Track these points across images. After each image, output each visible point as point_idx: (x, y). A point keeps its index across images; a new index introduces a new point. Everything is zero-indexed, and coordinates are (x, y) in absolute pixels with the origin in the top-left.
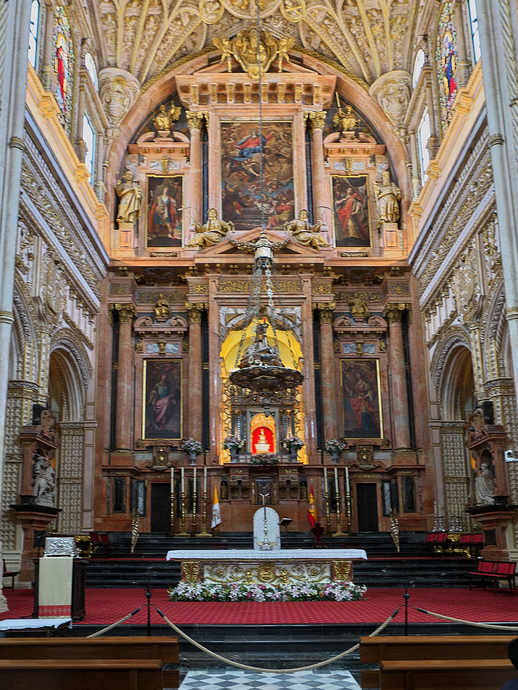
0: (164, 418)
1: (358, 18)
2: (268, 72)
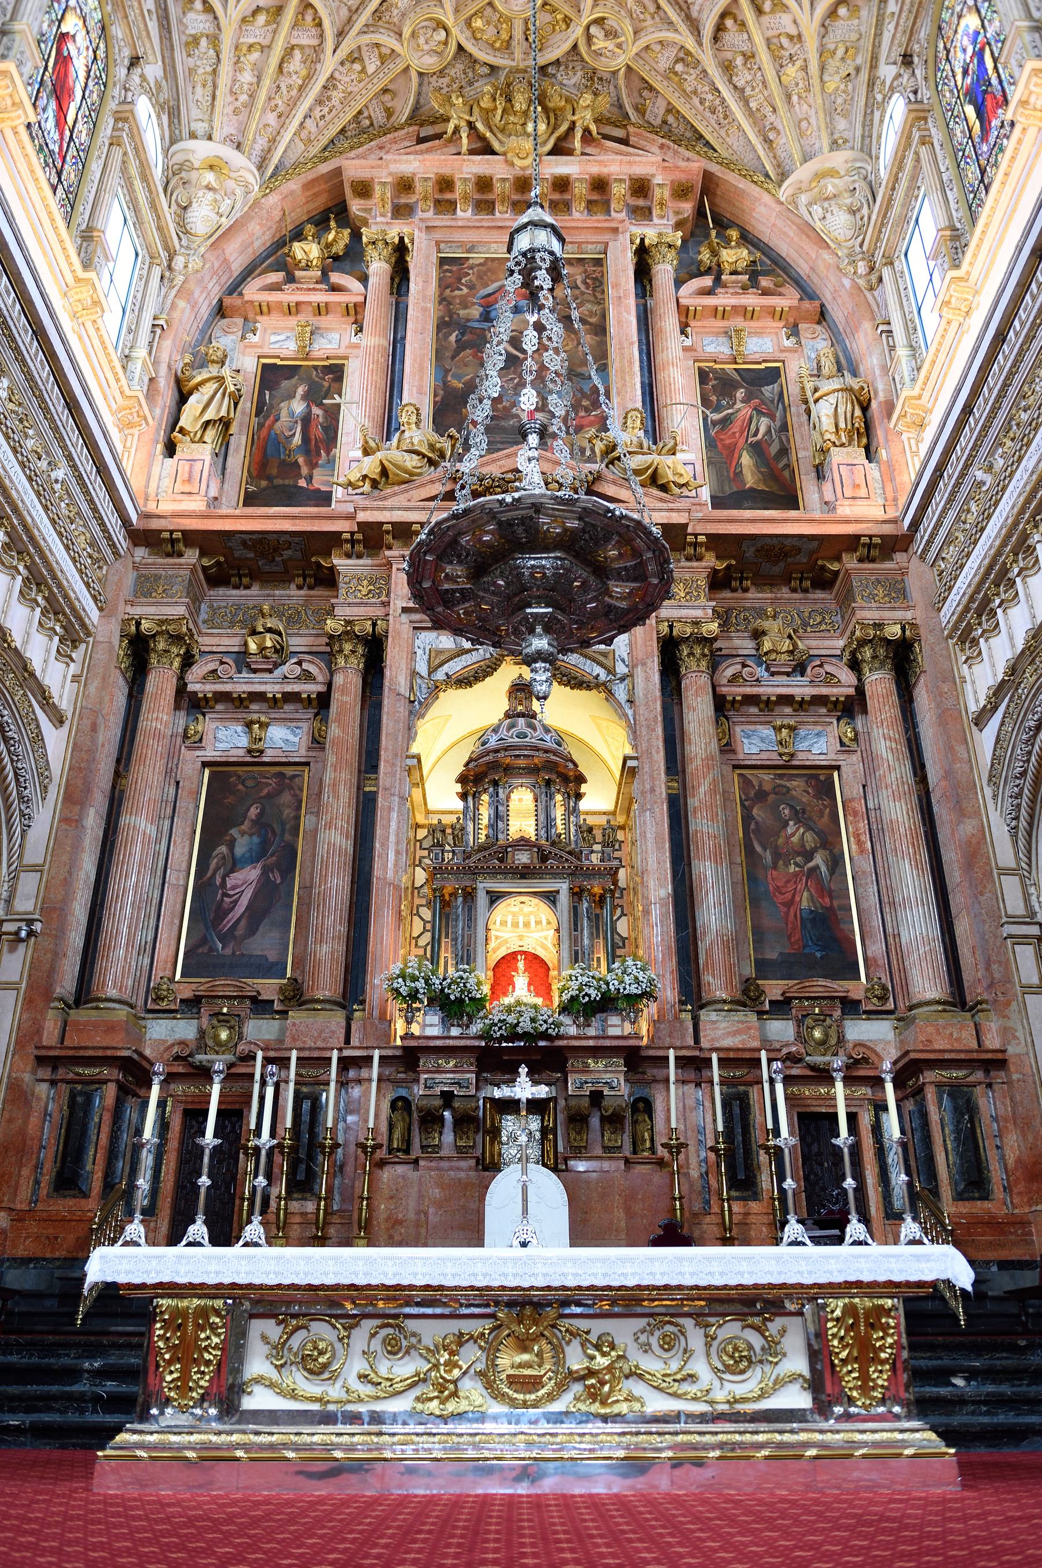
0: (243, 922)
1: (749, 57)
2: (551, 153)
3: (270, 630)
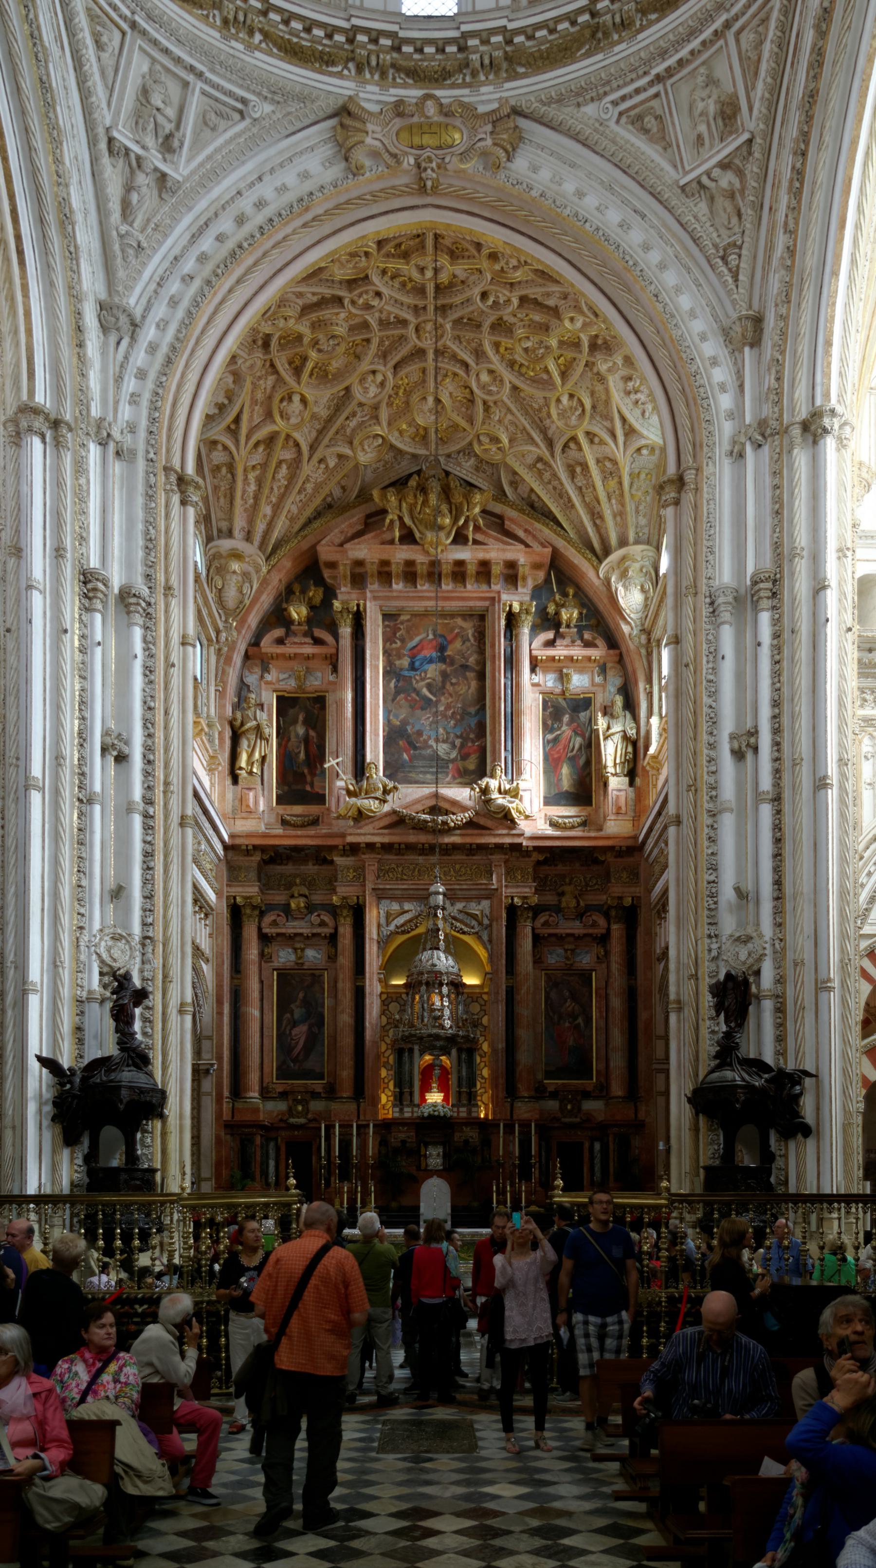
3: (301, 895)
